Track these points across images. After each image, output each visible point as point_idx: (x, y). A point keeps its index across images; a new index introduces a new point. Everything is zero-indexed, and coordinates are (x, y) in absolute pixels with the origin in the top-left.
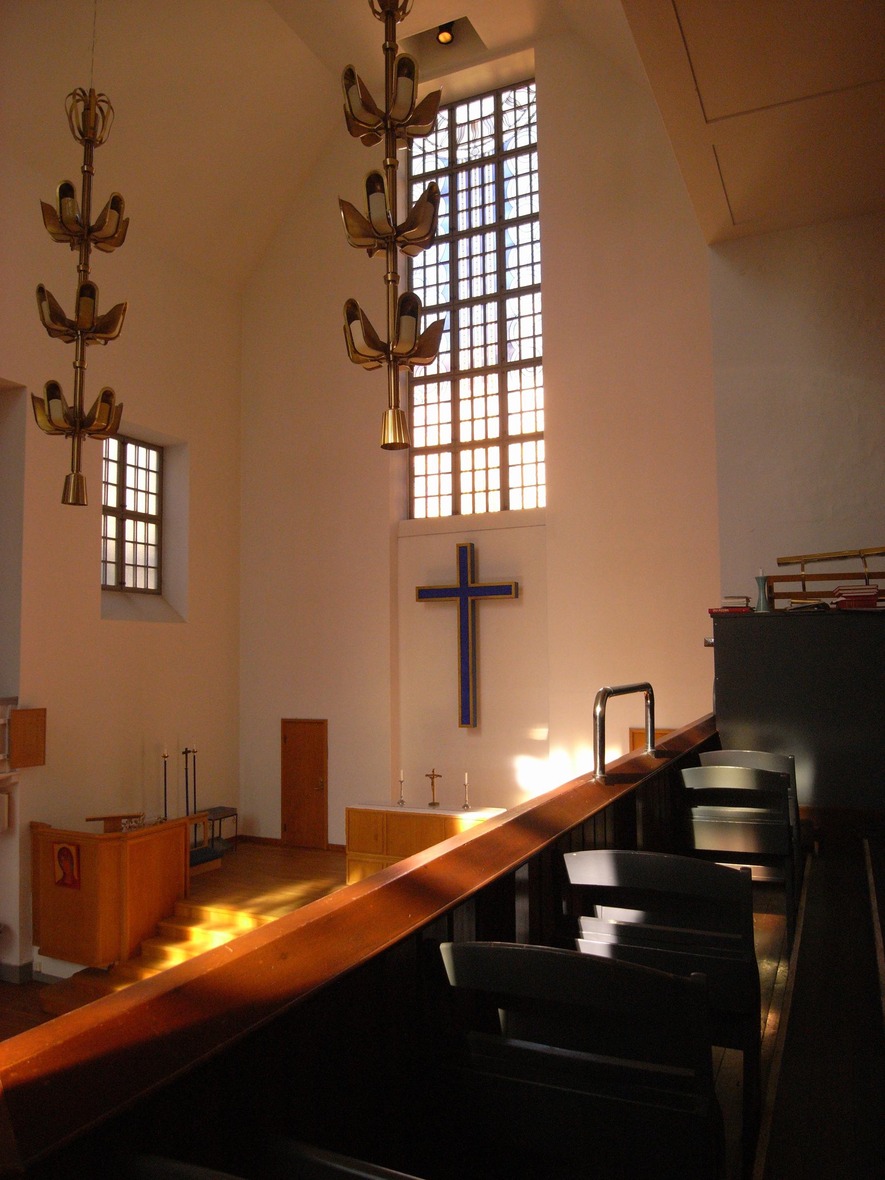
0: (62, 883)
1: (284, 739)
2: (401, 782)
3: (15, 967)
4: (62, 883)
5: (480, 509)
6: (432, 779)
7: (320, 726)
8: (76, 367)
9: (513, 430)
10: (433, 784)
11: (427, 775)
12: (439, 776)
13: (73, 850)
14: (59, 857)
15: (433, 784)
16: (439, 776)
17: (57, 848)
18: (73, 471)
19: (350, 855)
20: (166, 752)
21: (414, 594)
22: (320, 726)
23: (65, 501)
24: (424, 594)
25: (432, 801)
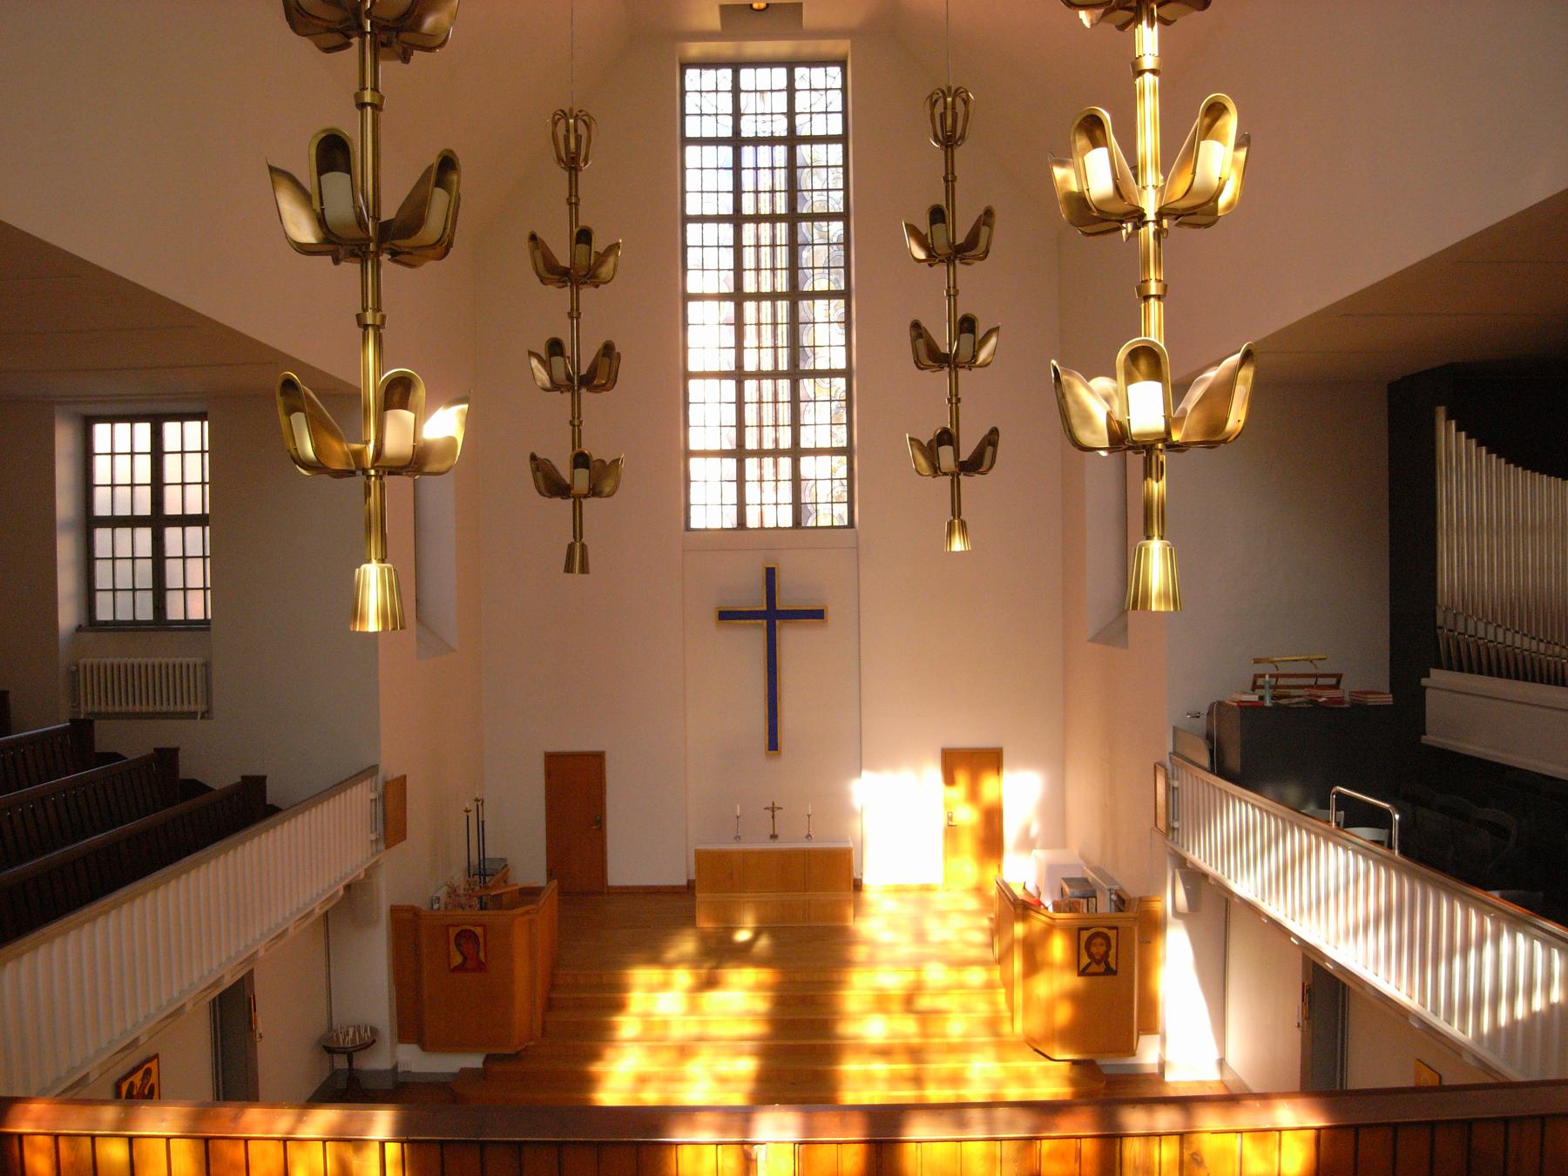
0: (461, 968)
1: (549, 775)
2: (738, 818)
3: (386, 1071)
4: (461, 968)
5: (769, 523)
6: (773, 811)
7: (597, 759)
8: (574, 426)
9: (805, 443)
10: (773, 817)
11: (766, 809)
12: (781, 808)
13: (479, 931)
14: (458, 945)
15: (773, 817)
16: (781, 808)
17: (453, 932)
18: (575, 537)
19: (701, 896)
20: (467, 806)
21: (714, 616)
22: (597, 759)
23: (569, 568)
24: (725, 616)
25: (772, 833)
